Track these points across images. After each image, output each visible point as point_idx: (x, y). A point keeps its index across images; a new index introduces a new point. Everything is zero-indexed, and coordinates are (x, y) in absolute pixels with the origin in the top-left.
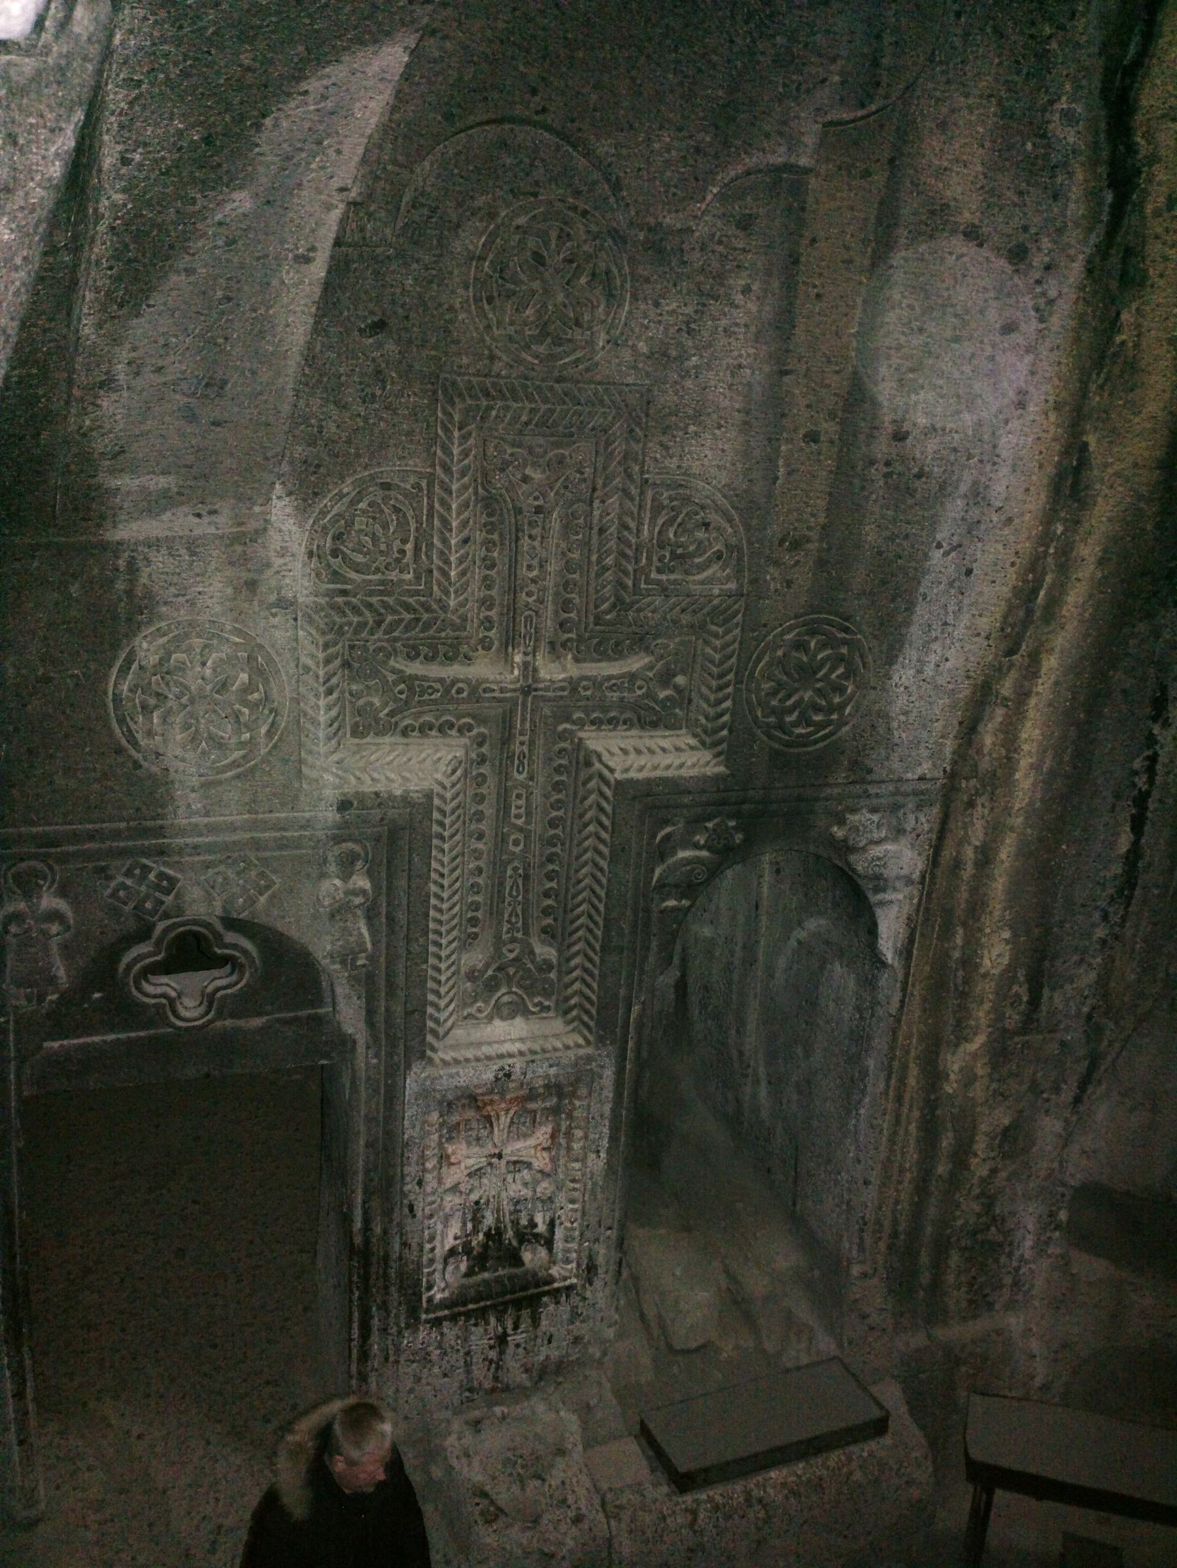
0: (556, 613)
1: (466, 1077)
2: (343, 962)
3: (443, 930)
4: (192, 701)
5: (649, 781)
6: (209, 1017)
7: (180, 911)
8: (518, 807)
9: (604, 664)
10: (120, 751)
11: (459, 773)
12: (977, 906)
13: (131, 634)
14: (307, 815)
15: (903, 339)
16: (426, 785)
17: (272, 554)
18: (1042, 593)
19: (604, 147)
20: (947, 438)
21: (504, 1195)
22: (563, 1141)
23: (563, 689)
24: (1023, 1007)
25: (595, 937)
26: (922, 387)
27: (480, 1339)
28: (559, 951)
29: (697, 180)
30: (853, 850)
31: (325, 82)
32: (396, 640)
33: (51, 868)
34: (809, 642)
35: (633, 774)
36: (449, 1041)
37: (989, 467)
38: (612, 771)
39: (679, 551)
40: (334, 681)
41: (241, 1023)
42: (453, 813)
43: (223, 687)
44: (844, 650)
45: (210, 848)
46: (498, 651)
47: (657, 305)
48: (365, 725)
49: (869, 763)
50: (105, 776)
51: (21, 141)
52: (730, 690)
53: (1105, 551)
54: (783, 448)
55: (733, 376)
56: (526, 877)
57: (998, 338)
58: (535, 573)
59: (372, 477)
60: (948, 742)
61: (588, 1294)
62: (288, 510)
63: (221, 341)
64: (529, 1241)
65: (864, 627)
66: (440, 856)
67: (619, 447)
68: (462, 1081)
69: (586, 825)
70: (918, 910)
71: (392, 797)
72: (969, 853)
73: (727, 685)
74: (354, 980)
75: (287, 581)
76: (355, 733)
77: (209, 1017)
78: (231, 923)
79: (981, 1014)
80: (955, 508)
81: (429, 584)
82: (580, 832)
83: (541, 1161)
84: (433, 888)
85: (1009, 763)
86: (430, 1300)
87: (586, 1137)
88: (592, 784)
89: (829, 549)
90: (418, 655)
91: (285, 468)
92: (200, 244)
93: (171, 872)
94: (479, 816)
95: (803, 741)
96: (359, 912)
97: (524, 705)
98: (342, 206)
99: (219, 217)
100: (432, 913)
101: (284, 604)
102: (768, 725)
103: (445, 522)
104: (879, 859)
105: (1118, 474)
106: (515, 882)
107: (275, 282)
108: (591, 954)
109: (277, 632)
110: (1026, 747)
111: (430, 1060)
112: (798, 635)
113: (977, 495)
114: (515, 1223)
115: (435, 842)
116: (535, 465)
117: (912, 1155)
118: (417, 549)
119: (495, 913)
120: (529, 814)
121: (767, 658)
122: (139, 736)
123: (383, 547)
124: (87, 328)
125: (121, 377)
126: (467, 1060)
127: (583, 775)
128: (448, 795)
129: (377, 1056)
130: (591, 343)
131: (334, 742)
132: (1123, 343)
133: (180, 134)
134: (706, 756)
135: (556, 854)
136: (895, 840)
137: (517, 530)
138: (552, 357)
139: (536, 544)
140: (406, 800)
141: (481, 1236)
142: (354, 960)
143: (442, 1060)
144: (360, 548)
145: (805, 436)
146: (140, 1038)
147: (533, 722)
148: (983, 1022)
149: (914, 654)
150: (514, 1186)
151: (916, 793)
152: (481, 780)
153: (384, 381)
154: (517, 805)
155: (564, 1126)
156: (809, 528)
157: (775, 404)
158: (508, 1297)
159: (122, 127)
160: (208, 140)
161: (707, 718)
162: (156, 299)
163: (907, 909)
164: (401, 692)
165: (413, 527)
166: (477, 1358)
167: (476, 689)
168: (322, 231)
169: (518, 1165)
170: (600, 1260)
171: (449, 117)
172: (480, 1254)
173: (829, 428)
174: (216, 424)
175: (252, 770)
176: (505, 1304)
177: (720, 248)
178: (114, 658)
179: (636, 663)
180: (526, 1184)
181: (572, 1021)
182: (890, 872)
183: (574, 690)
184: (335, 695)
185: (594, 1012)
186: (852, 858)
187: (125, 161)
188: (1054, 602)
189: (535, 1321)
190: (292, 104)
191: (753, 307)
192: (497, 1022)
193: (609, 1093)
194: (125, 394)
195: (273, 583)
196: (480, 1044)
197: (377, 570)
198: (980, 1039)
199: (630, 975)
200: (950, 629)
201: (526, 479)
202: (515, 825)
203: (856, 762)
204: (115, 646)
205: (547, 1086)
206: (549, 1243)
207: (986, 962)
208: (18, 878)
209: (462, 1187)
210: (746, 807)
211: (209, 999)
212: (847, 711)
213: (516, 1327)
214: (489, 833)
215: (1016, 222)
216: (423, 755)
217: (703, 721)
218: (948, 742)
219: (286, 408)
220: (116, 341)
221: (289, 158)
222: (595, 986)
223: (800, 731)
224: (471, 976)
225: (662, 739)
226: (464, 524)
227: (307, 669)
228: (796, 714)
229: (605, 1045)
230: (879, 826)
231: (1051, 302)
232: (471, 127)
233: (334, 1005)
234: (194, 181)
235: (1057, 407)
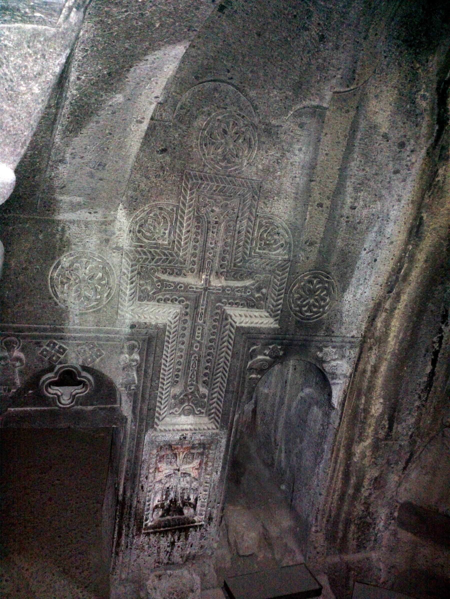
0: (219, 262)
1: (168, 437)
2: (126, 387)
3: (165, 378)
4: (80, 281)
5: (249, 328)
6: (72, 404)
7: (66, 362)
8: (198, 333)
9: (236, 282)
10: (50, 298)
11: (177, 318)
12: (371, 388)
13: (59, 255)
14: (118, 329)
15: (356, 172)
16: (164, 321)
17: (116, 230)
18: (403, 271)
19: (253, 94)
20: (370, 210)
21: (179, 486)
22: (204, 466)
23: (219, 290)
24: (386, 430)
25: (223, 386)
26: (362, 190)
27: (164, 542)
28: (209, 391)
29: (285, 108)
30: (324, 362)
31: (154, 57)
32: (158, 266)
33: (19, 341)
35: (243, 325)
36: (163, 422)
37: (385, 222)
38: (235, 323)
39: (268, 242)
40: (134, 279)
41: (84, 408)
42: (173, 333)
43: (92, 278)
44: (327, 285)
45: (80, 338)
46: (196, 273)
47: (267, 152)
48: (143, 297)
49: (333, 328)
50: (44, 307)
51: (47, 57)
52: (283, 296)
53: (427, 257)
54: (309, 208)
55: (293, 180)
56: (199, 361)
57: (392, 175)
58: (213, 246)
59: (156, 205)
60: (364, 324)
61: (208, 529)
62: (124, 214)
63: (106, 149)
64: (187, 505)
65: (335, 277)
66: (167, 349)
67: (248, 202)
68: (167, 439)
69: (223, 343)
70: (348, 388)
71: (151, 325)
72: (369, 368)
73: (281, 294)
74: (129, 395)
75: (120, 240)
76: (140, 299)
77: (72, 404)
78: (85, 368)
79: (370, 431)
80: (372, 236)
82: (221, 345)
83: (194, 474)
84: (163, 361)
85: (386, 334)
86: (146, 525)
87: (213, 465)
88: (227, 327)
89: (324, 247)
90: (166, 272)
91: (124, 198)
92: (102, 112)
93: (64, 346)
94: (183, 335)
95: (309, 318)
96: (134, 368)
97: (205, 294)
98: (155, 103)
99: (110, 103)
100: (162, 371)
101: (118, 248)
102: (296, 311)
103: (181, 223)
104: (335, 366)
105: (434, 229)
106: (195, 362)
107: (128, 129)
108: (221, 393)
109: (115, 259)
110: (393, 329)
111: (155, 430)
112: (310, 277)
113: (380, 232)
114: (182, 497)
115: (166, 343)
116: (217, 206)
117: (339, 485)
118: (170, 233)
119: (186, 374)
120: (202, 336)
121: (297, 285)
122: (58, 293)
123: (157, 231)
124: (57, 139)
125: (68, 159)
126: (170, 430)
127: (224, 323)
128: (173, 326)
129: (135, 425)
130: (241, 163)
131: (131, 302)
132: (439, 181)
133: (100, 70)
134: (272, 320)
136: (341, 359)
137: (208, 229)
138: (226, 167)
139: (214, 235)
140: (156, 326)
141: (168, 502)
142: (130, 387)
143: (160, 430)
144: (149, 230)
145: (318, 204)
146: (45, 410)
147: (207, 301)
148: (370, 434)
149: (353, 289)
150: (183, 483)
151: (350, 342)
152: (185, 321)
153: (164, 171)
154: (198, 332)
155: (204, 461)
156: (317, 239)
157: (308, 191)
158: (177, 527)
159: (79, 66)
160: (109, 74)
161: (273, 306)
162: (84, 131)
163: (344, 387)
164: (159, 286)
165: (169, 224)
166: (162, 550)
167: (187, 287)
168: (147, 113)
169: (185, 474)
170: (214, 515)
171: (197, 78)
172: (167, 509)
173: (327, 203)
174: (101, 179)
175: (100, 309)
176: (176, 530)
177: (292, 134)
178: (53, 263)
179: (248, 283)
180: (187, 482)
181: (212, 418)
182: (338, 372)
183: (224, 290)
184: (134, 284)
185: (220, 416)
186: (324, 365)
187: (79, 79)
188: (407, 275)
189: (187, 538)
190: (141, 64)
191: (302, 156)
192: (183, 417)
193: (223, 449)
194: (68, 165)
195: (115, 240)
196: (174, 424)
197: (154, 239)
198: (369, 441)
199: (235, 403)
200: (367, 281)
201: (213, 211)
202: (196, 340)
203: (328, 328)
204: (54, 258)
205: (199, 444)
206: (195, 507)
207: (373, 411)
208: (6, 343)
209: (163, 481)
210: (284, 341)
211: (73, 397)
212: (326, 308)
213: (179, 539)
215: (402, 133)
216: (165, 310)
217: (272, 307)
218: (364, 324)
219: (127, 176)
220: (67, 145)
221: (138, 84)
222: (222, 405)
223: (308, 314)
224: (174, 397)
225: (256, 312)
226: (189, 225)
227: (124, 274)
228: (307, 307)
229: (223, 429)
230: (335, 354)
231: (413, 163)
232: (204, 82)
233: (121, 404)
234: (102, 89)
235: (413, 202)
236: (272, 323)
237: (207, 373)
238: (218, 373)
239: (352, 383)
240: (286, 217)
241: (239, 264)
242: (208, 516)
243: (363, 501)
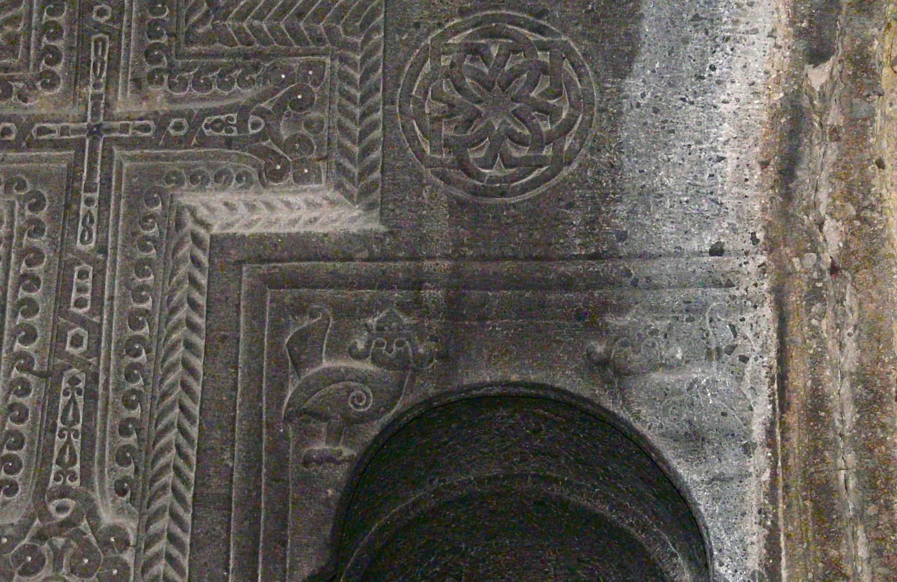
0: (141, 42)
25: (186, 482)
34: (486, 47)
35: (238, 230)
44: (543, 57)
94: (30, 307)
97: (93, 149)
120: (97, 300)
214: (43, 335)
222: (185, 563)
236: (353, 220)
237: (128, 448)
239: (779, 461)
241: (201, 30)
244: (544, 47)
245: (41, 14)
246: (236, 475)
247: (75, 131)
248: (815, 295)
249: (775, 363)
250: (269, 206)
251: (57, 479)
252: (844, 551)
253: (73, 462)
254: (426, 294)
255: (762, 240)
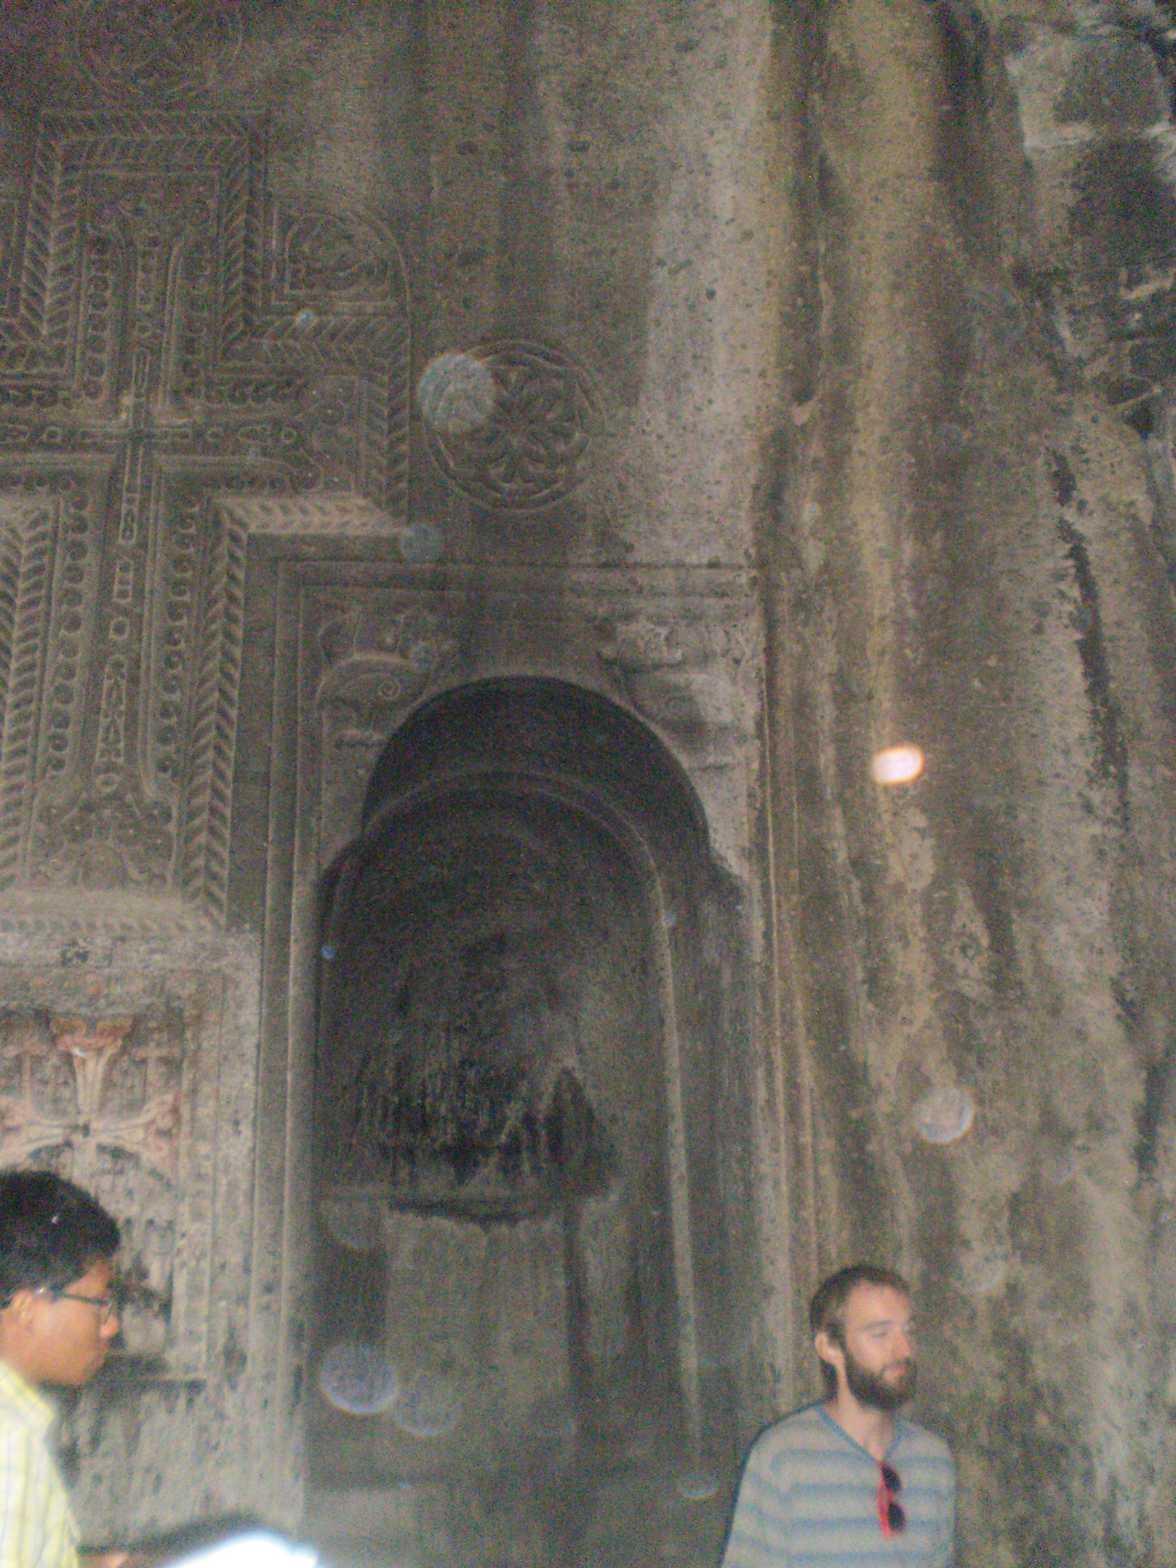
35: (273, 530)
38: (243, 525)
44: (560, 385)
49: (626, 536)
72: (824, 690)
81: (14, 309)
82: (205, 614)
106: (116, 684)
120: (139, 594)
135: (180, 654)
152: (77, 550)
161: (380, 470)
189: (133, 1438)
193: (250, 1015)
202: (117, 607)
207: (897, 871)
212: (580, 464)
213: (95, 1441)
218: (742, 513)
226: (65, 252)
229: (241, 931)
238: (201, 716)
239: (770, 753)
240: (364, 190)
242: (221, 1341)
243: (985, 1328)
244: (559, 376)
245: (86, 330)
246: (274, 756)
247: (117, 438)
248: (800, 605)
249: (763, 665)
250: (303, 511)
251: (103, 755)
252: (824, 829)
253: (118, 742)
254: (450, 594)
255: (754, 555)
